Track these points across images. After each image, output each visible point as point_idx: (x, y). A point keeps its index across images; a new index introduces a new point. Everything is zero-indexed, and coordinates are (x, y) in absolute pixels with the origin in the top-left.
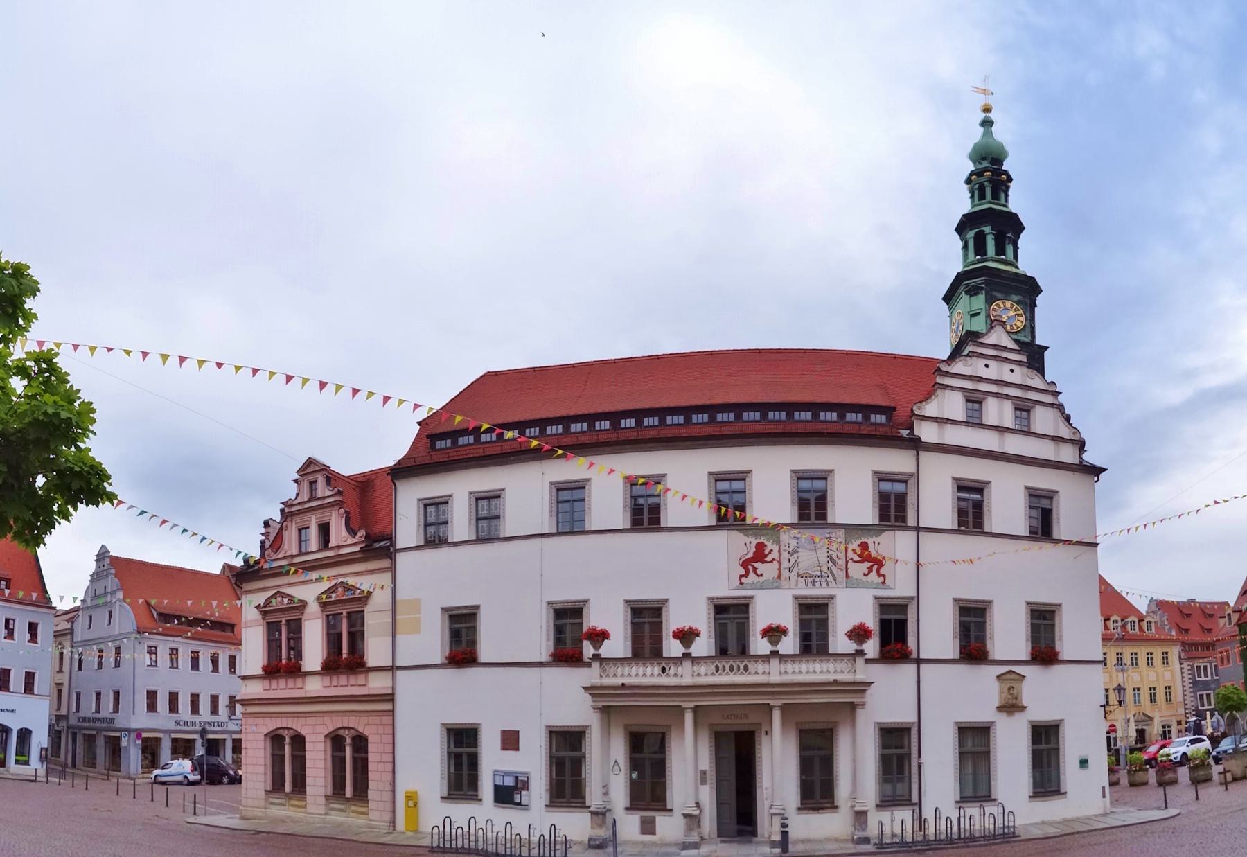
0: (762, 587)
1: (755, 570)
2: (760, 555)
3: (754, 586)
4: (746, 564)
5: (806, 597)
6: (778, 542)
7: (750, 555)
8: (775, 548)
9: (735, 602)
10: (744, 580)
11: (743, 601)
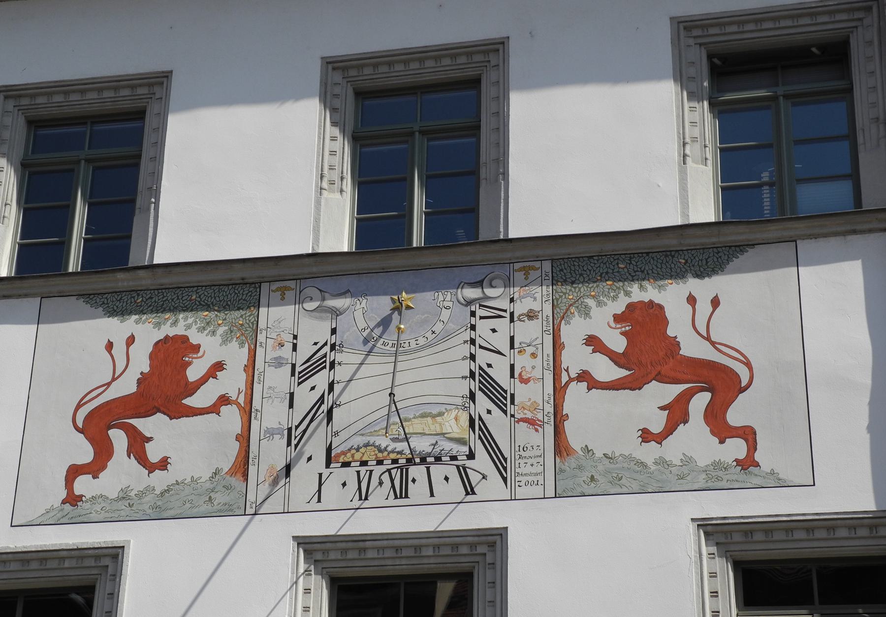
1: (138, 445)
7: (127, 386)
8: (235, 355)
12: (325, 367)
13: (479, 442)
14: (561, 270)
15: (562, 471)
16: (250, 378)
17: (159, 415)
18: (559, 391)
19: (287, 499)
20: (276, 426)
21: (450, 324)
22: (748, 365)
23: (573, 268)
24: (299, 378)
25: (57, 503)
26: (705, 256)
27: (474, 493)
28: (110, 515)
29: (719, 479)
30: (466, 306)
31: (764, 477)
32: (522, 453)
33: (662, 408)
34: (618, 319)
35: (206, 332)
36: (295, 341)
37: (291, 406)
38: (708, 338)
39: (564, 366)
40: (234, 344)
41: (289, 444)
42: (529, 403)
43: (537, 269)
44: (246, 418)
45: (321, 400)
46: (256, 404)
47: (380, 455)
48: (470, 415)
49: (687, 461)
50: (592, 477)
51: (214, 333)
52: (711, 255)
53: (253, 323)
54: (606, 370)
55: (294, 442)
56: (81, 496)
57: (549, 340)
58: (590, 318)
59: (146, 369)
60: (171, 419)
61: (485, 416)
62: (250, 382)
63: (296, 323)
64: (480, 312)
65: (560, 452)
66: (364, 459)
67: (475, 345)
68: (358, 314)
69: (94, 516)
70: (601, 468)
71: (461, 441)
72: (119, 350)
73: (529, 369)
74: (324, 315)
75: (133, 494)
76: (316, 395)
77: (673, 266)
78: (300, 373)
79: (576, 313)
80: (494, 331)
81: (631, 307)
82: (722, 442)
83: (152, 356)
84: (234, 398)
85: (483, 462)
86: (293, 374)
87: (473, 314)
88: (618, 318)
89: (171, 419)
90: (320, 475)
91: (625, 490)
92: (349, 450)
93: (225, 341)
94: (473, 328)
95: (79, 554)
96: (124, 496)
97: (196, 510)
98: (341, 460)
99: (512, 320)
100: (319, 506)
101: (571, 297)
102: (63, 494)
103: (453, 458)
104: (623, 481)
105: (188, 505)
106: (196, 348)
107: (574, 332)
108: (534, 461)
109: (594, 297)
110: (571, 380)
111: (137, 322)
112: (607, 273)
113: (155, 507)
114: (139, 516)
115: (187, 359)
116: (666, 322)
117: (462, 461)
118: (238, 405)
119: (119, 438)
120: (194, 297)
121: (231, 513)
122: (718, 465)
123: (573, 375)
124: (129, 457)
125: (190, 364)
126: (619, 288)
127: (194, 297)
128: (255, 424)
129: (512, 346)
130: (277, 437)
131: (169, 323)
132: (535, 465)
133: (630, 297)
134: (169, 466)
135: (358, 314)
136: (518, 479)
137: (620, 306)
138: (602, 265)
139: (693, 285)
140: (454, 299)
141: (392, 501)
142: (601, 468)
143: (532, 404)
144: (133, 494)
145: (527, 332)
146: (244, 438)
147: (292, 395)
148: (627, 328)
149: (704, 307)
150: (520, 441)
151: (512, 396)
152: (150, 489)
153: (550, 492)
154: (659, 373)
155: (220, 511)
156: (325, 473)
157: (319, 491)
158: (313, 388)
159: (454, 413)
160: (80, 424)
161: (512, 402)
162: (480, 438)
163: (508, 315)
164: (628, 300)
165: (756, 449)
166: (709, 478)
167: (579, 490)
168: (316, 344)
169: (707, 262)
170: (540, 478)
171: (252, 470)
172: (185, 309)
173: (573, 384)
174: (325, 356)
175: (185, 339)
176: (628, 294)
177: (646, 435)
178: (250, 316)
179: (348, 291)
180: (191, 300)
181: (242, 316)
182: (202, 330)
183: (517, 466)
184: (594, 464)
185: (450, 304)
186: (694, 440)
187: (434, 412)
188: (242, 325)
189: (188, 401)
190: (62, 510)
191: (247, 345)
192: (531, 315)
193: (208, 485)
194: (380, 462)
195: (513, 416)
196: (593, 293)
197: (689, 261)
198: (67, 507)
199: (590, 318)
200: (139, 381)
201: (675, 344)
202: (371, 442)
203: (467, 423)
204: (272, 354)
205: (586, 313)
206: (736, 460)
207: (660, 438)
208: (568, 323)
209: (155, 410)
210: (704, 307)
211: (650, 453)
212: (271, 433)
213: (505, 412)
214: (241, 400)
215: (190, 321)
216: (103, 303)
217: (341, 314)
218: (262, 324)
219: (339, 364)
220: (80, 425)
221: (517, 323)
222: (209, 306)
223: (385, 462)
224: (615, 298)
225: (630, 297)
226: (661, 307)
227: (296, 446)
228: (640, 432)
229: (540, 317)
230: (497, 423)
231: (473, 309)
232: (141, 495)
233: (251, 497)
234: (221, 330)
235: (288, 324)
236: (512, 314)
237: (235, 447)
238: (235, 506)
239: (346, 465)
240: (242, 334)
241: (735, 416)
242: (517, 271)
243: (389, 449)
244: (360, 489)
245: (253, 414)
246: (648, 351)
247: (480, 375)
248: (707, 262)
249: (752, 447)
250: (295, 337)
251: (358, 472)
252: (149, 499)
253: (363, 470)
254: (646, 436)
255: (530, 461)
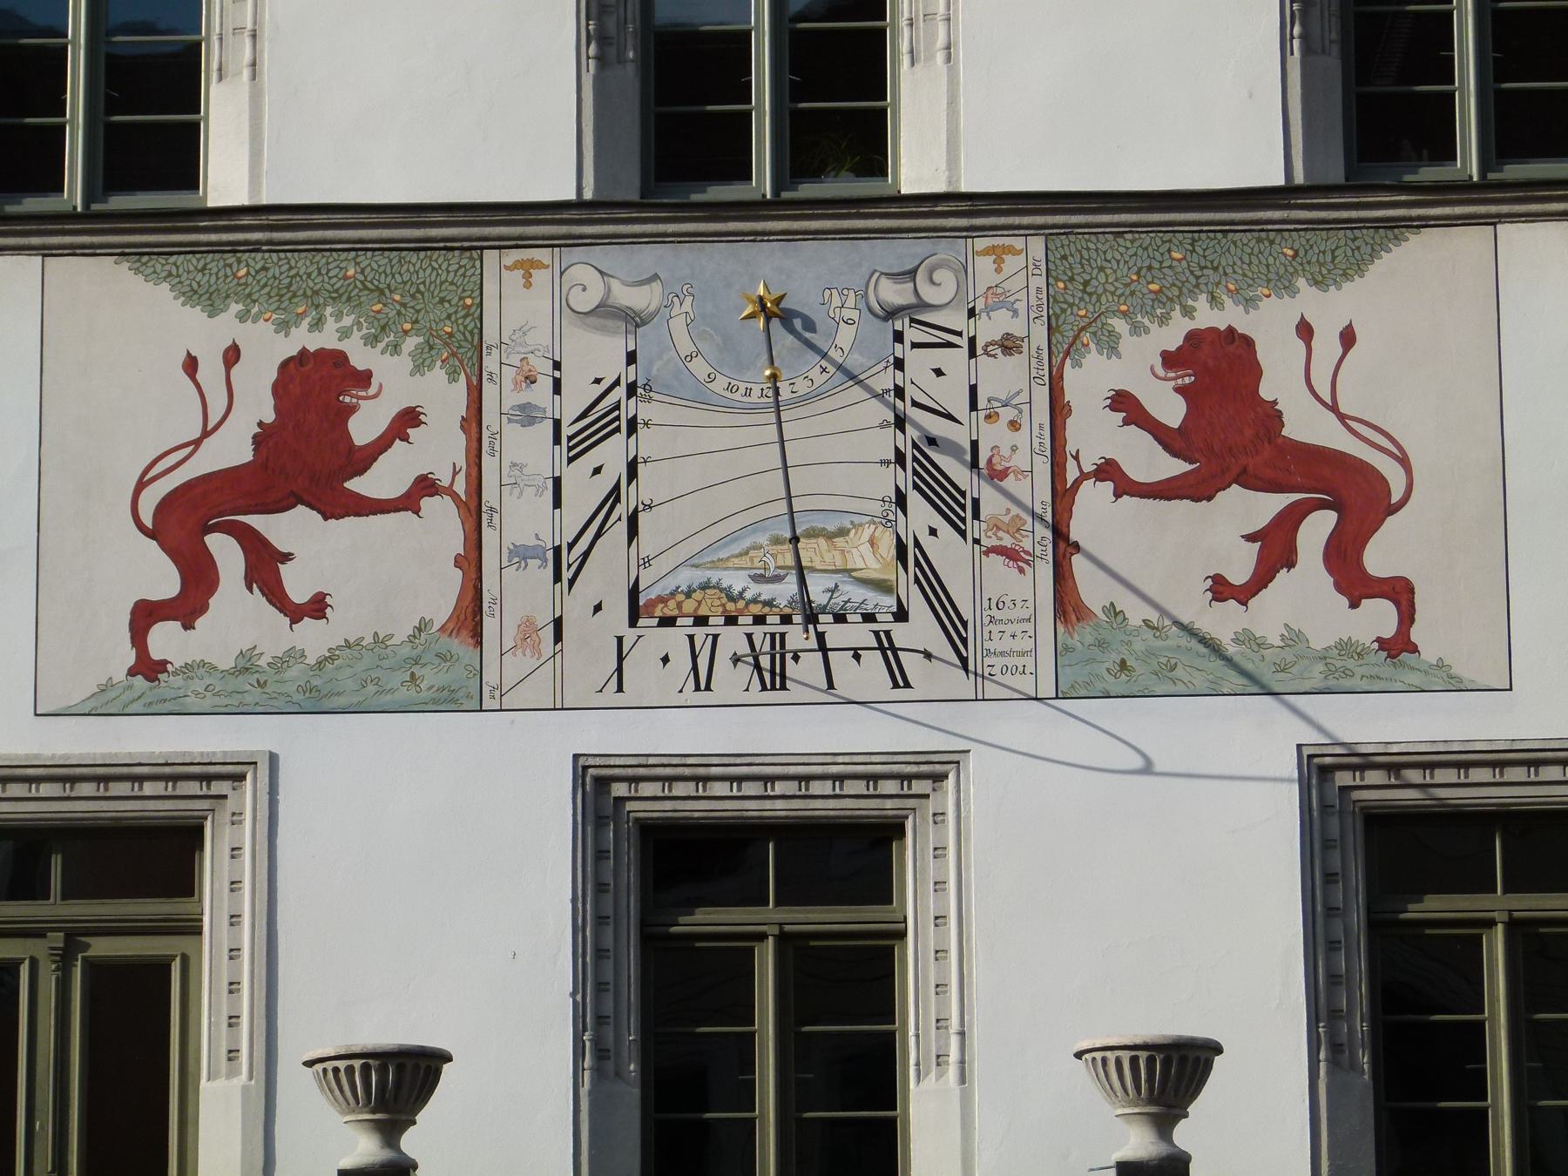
0: (316, 698)
1: (264, 566)
2: (310, 451)
3: (252, 687)
4: (187, 520)
5: (699, 771)
6: (465, 350)
7: (232, 449)
9: (85, 805)
10: (165, 639)
11: (153, 803)
12: (618, 430)
13: (915, 589)
14: (1064, 257)
15: (1067, 649)
16: (475, 444)
17: (301, 509)
18: (1063, 496)
19: (559, 681)
20: (533, 542)
21: (856, 356)
22: (1404, 461)
23: (1085, 253)
24: (570, 449)
25: (120, 675)
26: (1331, 245)
27: (907, 685)
28: (223, 701)
29: (1347, 673)
30: (885, 319)
31: (1426, 673)
32: (994, 612)
33: (1251, 538)
34: (1170, 360)
35: (381, 346)
36: (557, 374)
37: (557, 503)
38: (1334, 408)
39: (1071, 448)
40: (438, 374)
41: (557, 577)
42: (1006, 519)
43: (1019, 253)
44: (471, 523)
45: (615, 494)
46: (489, 495)
47: (730, 606)
48: (898, 537)
49: (1293, 638)
50: (1123, 662)
51: (395, 349)
52: (1342, 243)
53: (471, 332)
54: (1149, 461)
55: (567, 575)
56: (164, 663)
57: (1042, 395)
58: (1119, 356)
59: (269, 416)
60: (326, 519)
61: (925, 540)
62: (474, 452)
63: (558, 336)
64: (913, 334)
65: (1065, 613)
66: (703, 612)
67: (903, 400)
68: (678, 325)
69: (192, 702)
70: (1138, 646)
71: (883, 587)
72: (211, 370)
73: (1005, 452)
74: (610, 323)
75: (263, 662)
76: (604, 484)
77: (1271, 260)
78: (570, 438)
79: (1092, 346)
80: (939, 372)
81: (1193, 337)
82: (1354, 605)
83: (278, 389)
84: (445, 483)
85: (922, 630)
86: (557, 440)
87: (899, 337)
88: (1169, 360)
89: (326, 519)
90: (620, 640)
91: (1181, 688)
92: (673, 594)
93: (419, 368)
94: (899, 364)
95: (172, 773)
96: (246, 665)
97: (389, 697)
98: (658, 613)
99: (972, 354)
100: (620, 700)
101: (1082, 313)
102: (130, 658)
103: (869, 618)
104: (1179, 672)
105: (371, 688)
106: (364, 378)
107: (1090, 380)
108: (1017, 628)
109: (1124, 314)
110: (1084, 476)
111: (242, 317)
112: (1150, 268)
113: (308, 689)
114: (280, 704)
115: (347, 399)
116: (1256, 372)
117: (885, 622)
118: (455, 496)
119: (225, 551)
120: (351, 272)
121: (454, 707)
122: (1347, 648)
123: (1088, 468)
124: (250, 589)
125: (352, 409)
126: (1171, 300)
127: (351, 272)
128: (489, 537)
129: (973, 406)
130: (534, 563)
131: (306, 323)
132: (1020, 635)
133: (1192, 318)
134: (328, 610)
135: (678, 325)
136: (987, 661)
137: (1172, 336)
138: (1140, 251)
139: (1308, 300)
140: (862, 305)
141: (755, 694)
142: (1138, 646)
143: (1013, 519)
144: (263, 662)
145: (1003, 377)
146: (471, 561)
147: (557, 482)
148: (1187, 380)
149: (1327, 344)
150: (991, 591)
151: (976, 502)
152: (293, 655)
153: (1047, 689)
154: (1245, 470)
155: (434, 701)
156: (630, 635)
157: (620, 670)
158: (597, 471)
159: (867, 532)
160: (148, 521)
161: (976, 516)
162: (917, 581)
163: (964, 342)
164: (1188, 325)
165: (1412, 621)
166: (1330, 672)
167: (1099, 687)
168: (598, 381)
169: (1334, 258)
170: (1029, 661)
171: (490, 625)
172: (335, 297)
173: (1088, 485)
174: (617, 407)
175: (338, 359)
176: (1188, 312)
177: (1221, 589)
178: (465, 317)
179: (655, 277)
180: (345, 278)
181: (449, 317)
182: (371, 340)
183: (986, 636)
184: (1126, 638)
185: (855, 315)
186: (1304, 599)
187: (831, 528)
188: (451, 335)
189: (355, 485)
190: (130, 687)
191: (463, 375)
192: (1008, 345)
193: (406, 651)
194: (731, 621)
195: (977, 541)
196: (1124, 308)
197: (1302, 253)
198: (139, 680)
199: (1119, 356)
200: (257, 440)
201: (1272, 416)
202: (714, 581)
203: (893, 552)
204: (513, 399)
205: (1111, 346)
206: (1379, 640)
207: (1245, 594)
208: (1077, 364)
209: (292, 500)
210: (1327, 344)
211: (1223, 622)
212: (521, 555)
213: (963, 534)
214: (460, 487)
215: (347, 321)
216: (170, 274)
217: (644, 323)
218: (490, 336)
219: (646, 424)
220: (148, 521)
221: (982, 359)
222: (382, 292)
223: (741, 620)
224: (1164, 320)
225: (1192, 318)
226: (1248, 343)
227: (572, 582)
228: (1210, 582)
229: (1025, 349)
230: (949, 554)
231: (898, 327)
232: (280, 664)
233: (491, 677)
234: (411, 343)
235: (540, 337)
236: (972, 341)
237: (455, 579)
238: (460, 694)
239: (667, 622)
240: (454, 354)
241: (1379, 558)
242: (979, 253)
243: (748, 595)
244: (695, 668)
245: (485, 517)
246: (1223, 427)
247: (915, 459)
248: (1334, 258)
249: (1407, 616)
250: (557, 366)
251: (691, 638)
252: (294, 672)
253: (700, 632)
254: (1220, 589)
255: (1009, 629)
